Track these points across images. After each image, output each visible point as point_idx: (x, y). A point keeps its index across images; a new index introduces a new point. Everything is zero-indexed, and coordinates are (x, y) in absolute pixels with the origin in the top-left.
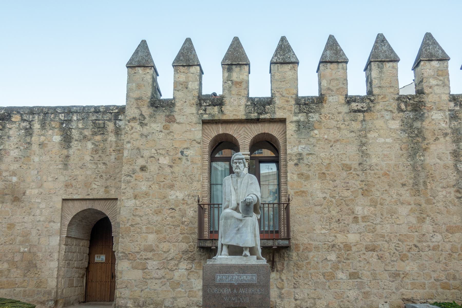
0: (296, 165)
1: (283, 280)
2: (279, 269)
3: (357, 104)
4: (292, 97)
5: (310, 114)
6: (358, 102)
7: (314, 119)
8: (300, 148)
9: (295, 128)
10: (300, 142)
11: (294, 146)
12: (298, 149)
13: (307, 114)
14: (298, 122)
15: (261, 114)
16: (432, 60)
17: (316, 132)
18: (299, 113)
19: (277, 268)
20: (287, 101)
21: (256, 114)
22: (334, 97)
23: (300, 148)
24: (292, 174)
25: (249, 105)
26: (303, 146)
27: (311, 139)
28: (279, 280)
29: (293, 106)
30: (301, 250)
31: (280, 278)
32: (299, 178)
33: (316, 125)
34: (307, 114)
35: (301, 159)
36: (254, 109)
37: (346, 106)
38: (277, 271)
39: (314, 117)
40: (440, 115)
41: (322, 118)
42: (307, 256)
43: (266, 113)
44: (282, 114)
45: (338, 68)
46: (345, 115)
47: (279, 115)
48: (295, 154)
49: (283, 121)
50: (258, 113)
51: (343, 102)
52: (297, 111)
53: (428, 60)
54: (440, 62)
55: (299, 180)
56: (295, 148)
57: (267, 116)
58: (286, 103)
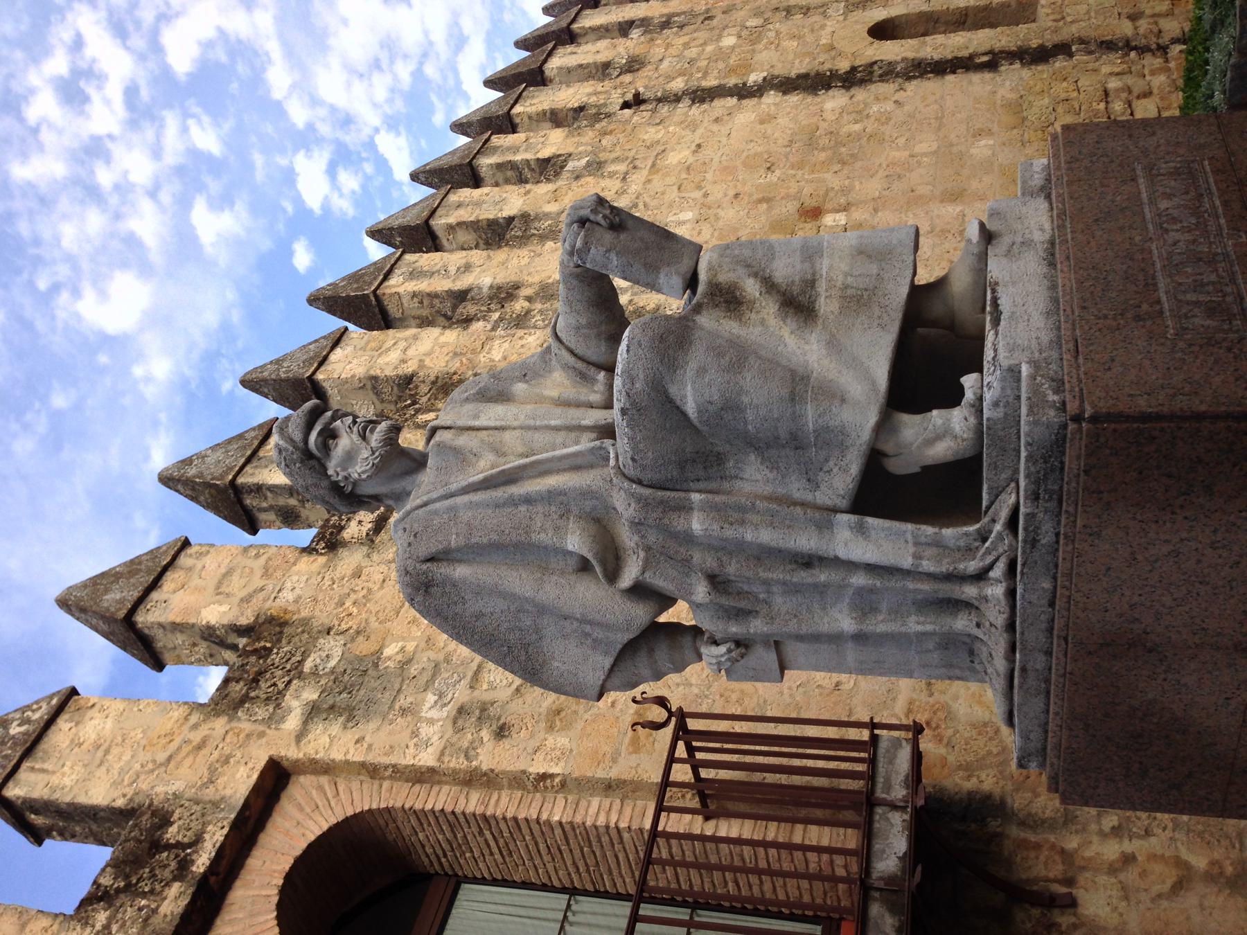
0: (502, 732)
1: (1128, 859)
2: (1057, 870)
3: (353, 524)
4: (195, 727)
5: (308, 666)
6: (349, 520)
7: (337, 653)
8: (434, 714)
9: (335, 728)
10: (404, 712)
11: (415, 734)
12: (431, 722)
13: (300, 676)
14: (313, 712)
15: (184, 865)
16: (325, 358)
17: (390, 650)
18: (278, 706)
19: (1048, 880)
20: (200, 747)
21: (176, 887)
22: (289, 585)
23: (434, 714)
24: (540, 756)
25: (110, 921)
26: (431, 698)
27: (413, 670)
28: (1130, 876)
29: (234, 724)
30: (943, 751)
31: (1113, 870)
32: (567, 727)
33: (363, 647)
34: (300, 676)
35: (483, 709)
36: (144, 895)
37: (343, 553)
38: (1070, 882)
39: (329, 653)
40: (496, 347)
41: (344, 626)
42: (973, 726)
43: (197, 841)
44: (242, 772)
45: (190, 569)
46: (375, 557)
47: (239, 783)
48: (450, 732)
49: (276, 778)
50: (175, 879)
51: (322, 560)
52: (262, 712)
53: (321, 364)
54: (342, 344)
55: (579, 725)
56: (425, 731)
57: (215, 836)
58: (203, 752)
